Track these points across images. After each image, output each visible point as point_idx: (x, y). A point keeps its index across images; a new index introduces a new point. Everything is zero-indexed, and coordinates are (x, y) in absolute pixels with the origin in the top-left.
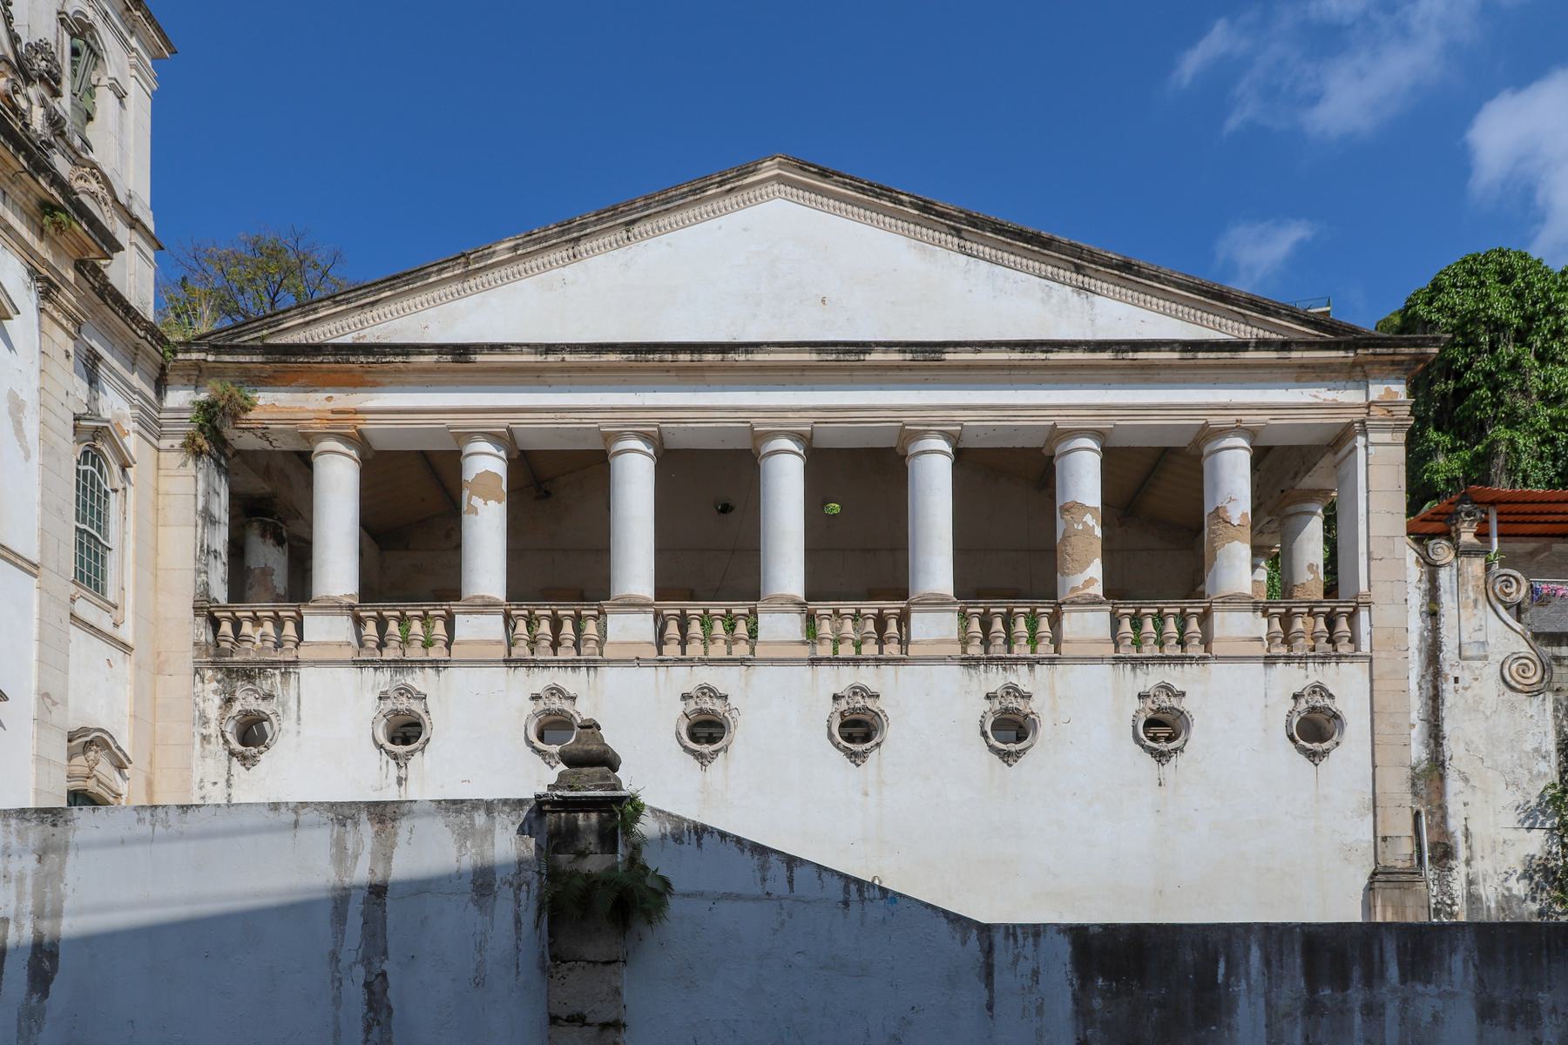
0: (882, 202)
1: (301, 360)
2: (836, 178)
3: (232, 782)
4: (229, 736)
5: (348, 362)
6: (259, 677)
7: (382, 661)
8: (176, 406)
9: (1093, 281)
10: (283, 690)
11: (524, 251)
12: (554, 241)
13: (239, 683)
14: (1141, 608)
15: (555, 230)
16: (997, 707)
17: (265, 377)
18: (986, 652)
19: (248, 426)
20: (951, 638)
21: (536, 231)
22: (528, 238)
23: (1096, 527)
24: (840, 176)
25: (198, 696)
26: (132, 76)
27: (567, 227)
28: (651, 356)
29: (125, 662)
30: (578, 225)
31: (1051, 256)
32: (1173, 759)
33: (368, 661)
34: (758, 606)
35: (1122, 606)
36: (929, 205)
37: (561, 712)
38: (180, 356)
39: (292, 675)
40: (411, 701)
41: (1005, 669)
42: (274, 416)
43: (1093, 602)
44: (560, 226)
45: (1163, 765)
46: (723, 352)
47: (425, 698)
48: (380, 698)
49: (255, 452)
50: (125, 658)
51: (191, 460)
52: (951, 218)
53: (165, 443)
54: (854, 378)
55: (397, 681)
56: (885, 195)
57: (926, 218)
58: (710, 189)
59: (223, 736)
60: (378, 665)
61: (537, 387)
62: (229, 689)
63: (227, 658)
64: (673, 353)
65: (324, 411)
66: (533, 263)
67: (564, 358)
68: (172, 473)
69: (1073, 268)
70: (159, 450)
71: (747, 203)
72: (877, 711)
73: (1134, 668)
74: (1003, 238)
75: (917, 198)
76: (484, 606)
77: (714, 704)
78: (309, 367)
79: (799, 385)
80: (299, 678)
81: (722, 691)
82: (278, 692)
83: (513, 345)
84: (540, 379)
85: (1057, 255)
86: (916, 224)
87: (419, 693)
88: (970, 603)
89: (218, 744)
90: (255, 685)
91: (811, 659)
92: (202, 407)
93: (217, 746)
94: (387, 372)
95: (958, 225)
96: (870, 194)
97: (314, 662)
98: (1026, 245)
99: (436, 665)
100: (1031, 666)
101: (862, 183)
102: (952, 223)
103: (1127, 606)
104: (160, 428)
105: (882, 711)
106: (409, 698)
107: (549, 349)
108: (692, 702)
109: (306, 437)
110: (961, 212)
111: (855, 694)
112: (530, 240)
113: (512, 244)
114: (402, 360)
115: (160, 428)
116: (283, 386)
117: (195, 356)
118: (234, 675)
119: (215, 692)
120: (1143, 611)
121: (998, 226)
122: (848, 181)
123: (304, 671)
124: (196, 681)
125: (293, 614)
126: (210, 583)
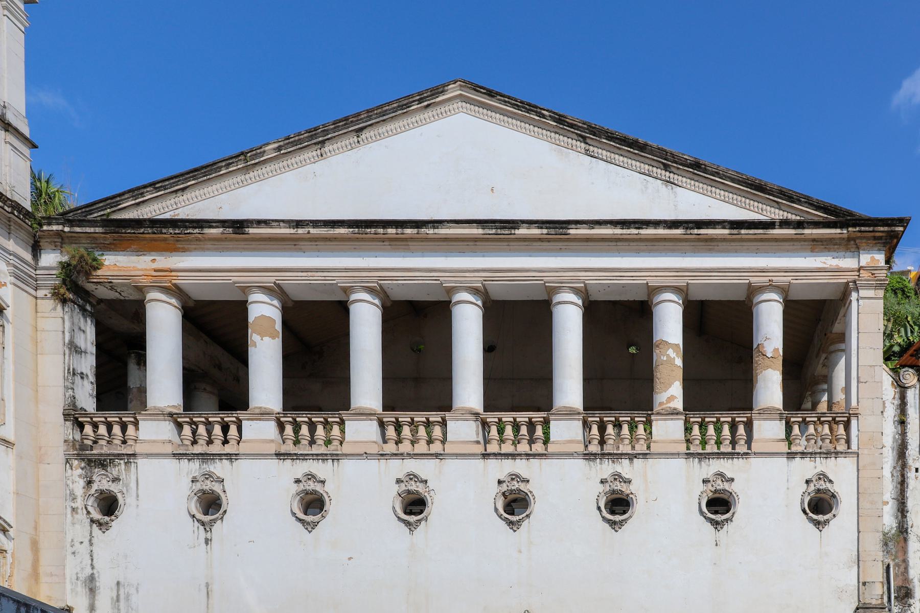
0: (532, 116)
1: (129, 231)
2: (499, 97)
3: (93, 542)
4: (90, 509)
5: (162, 233)
6: (110, 466)
7: (192, 454)
8: (48, 265)
9: (676, 176)
10: (126, 475)
11: (286, 151)
12: (306, 144)
13: (97, 470)
14: (705, 417)
15: (306, 135)
16: (608, 489)
17: (108, 244)
18: (602, 449)
19: (98, 280)
20: (577, 439)
21: (292, 136)
22: (287, 141)
23: (676, 358)
24: (501, 96)
25: (68, 479)
26: (4, 15)
27: (314, 133)
28: (369, 230)
29: (7, 454)
30: (321, 131)
31: (647, 158)
32: (725, 527)
33: (183, 454)
34: (446, 415)
35: (692, 416)
36: (563, 118)
37: (314, 492)
38: (45, 228)
39: (132, 464)
40: (213, 483)
41: (613, 462)
42: (115, 273)
43: (674, 413)
44: (309, 132)
45: (719, 531)
46: (418, 227)
47: (223, 481)
48: (193, 481)
49: (113, 300)
50: (7, 451)
51: (59, 305)
52: (578, 128)
53: (41, 293)
54: (511, 247)
55: (204, 469)
56: (533, 111)
57: (562, 128)
58: (413, 105)
59: (86, 509)
60: (191, 457)
61: (296, 253)
62: (89, 474)
63: (87, 452)
64: (384, 227)
65: (148, 270)
66: (293, 160)
67: (309, 231)
68: (46, 315)
69: (662, 167)
70: (36, 298)
71: (441, 116)
72: (526, 491)
73: (700, 462)
74: (613, 144)
75: (554, 113)
76: (261, 414)
77: (417, 487)
78: (137, 237)
79: (474, 252)
80: (137, 466)
81: (424, 478)
82: (123, 476)
83: (273, 221)
84: (296, 247)
85: (650, 156)
86: (556, 133)
87: (218, 478)
88: (590, 414)
89: (83, 514)
90: (107, 471)
91: (483, 454)
92: (64, 266)
93: (82, 516)
94: (191, 241)
95: (584, 134)
96: (523, 109)
97: (147, 454)
98: (629, 149)
99: (230, 457)
100: (631, 459)
101: (517, 101)
102: (579, 132)
103: (696, 416)
104: (36, 281)
105: (531, 492)
106: (212, 481)
107: (299, 224)
108: (403, 485)
109: (140, 290)
110: (584, 124)
111: (513, 479)
112: (289, 143)
113: (276, 145)
114: (198, 232)
115: (36, 281)
116: (121, 251)
117: (55, 228)
118: (93, 464)
119: (80, 476)
120: (707, 420)
121: (609, 134)
122: (507, 99)
123: (140, 461)
124: (67, 469)
125: (132, 419)
126: (77, 397)
